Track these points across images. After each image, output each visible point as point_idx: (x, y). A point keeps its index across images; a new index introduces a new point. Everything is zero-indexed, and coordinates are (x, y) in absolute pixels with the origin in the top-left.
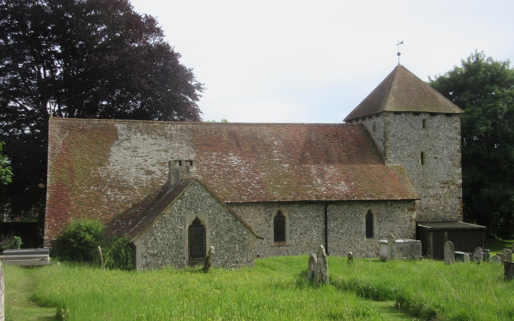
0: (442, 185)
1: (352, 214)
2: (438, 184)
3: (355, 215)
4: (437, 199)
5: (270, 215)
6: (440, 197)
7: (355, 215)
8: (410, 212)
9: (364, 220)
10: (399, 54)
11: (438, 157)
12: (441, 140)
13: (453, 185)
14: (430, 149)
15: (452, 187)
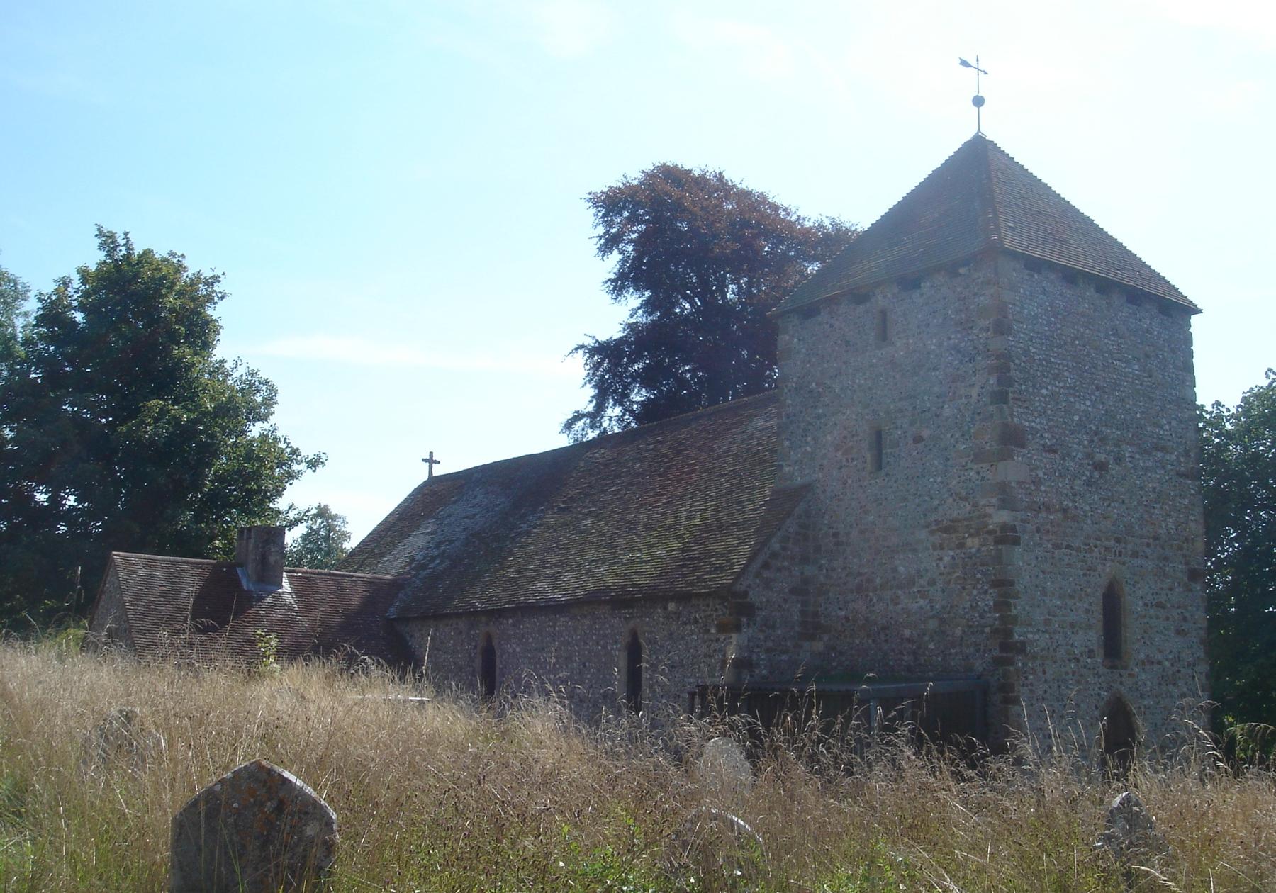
0: (936, 539)
1: (598, 644)
2: (923, 534)
3: (604, 647)
4: (922, 594)
5: (475, 647)
6: (932, 583)
7: (604, 647)
8: (722, 637)
9: (622, 659)
10: (978, 101)
11: (926, 433)
12: (935, 369)
13: (977, 533)
14: (901, 411)
15: (973, 543)
